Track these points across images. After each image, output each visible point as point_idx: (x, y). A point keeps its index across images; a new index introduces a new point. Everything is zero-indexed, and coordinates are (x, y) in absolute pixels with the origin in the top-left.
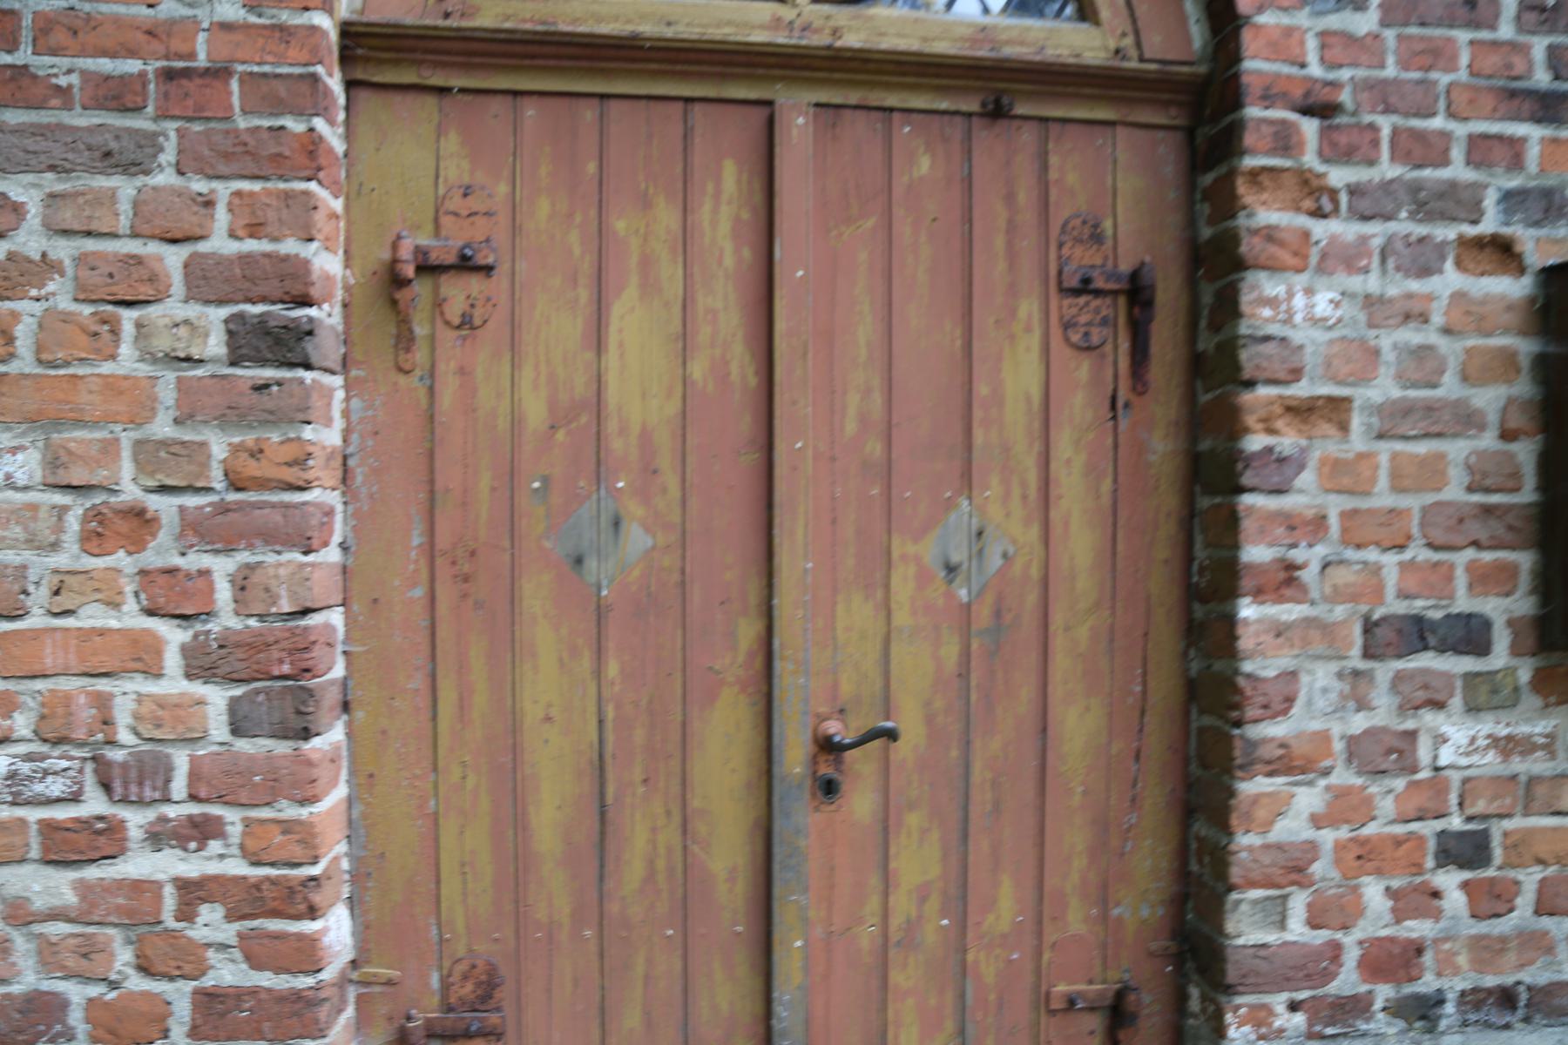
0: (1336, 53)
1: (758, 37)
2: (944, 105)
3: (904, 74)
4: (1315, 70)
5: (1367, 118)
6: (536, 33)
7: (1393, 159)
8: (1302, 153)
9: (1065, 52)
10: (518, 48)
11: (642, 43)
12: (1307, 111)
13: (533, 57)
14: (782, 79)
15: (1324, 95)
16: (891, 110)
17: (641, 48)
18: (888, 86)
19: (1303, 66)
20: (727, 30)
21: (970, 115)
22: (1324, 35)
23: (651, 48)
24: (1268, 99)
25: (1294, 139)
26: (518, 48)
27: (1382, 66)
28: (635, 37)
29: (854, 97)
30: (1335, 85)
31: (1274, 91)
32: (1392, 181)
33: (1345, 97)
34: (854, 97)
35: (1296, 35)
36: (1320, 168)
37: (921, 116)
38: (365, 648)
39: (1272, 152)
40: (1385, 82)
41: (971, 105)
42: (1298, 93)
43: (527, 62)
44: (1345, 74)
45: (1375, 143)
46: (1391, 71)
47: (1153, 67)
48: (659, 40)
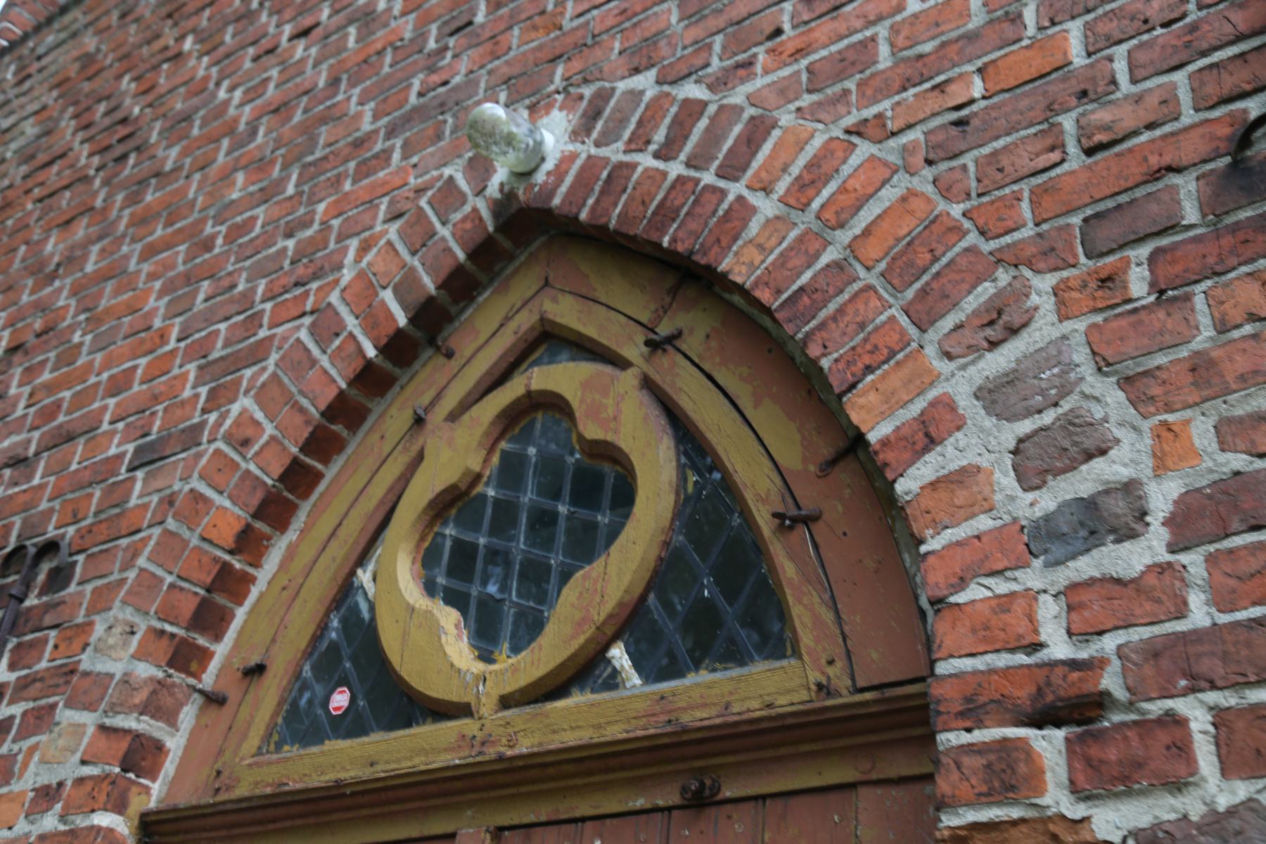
0: (1096, 612)
1: (440, 761)
2: (640, 803)
3: (590, 773)
4: (1059, 648)
5: (1155, 708)
6: (266, 796)
7: (1227, 771)
8: (1040, 790)
9: (755, 704)
10: (259, 815)
11: (342, 791)
12: (1040, 720)
13: (274, 821)
14: (470, 804)
15: (1073, 684)
16: (583, 820)
17: (344, 795)
18: (578, 790)
19: (1037, 646)
20: (699, 714)
21: (669, 809)
22: (1073, 595)
23: (353, 794)
24: (972, 715)
25: (1022, 768)
26: (259, 815)
27: (1181, 611)
28: (338, 784)
29: (543, 812)
30: (1094, 665)
31: (982, 699)
32: (1232, 812)
33: (1111, 682)
34: (543, 812)
35: (1019, 607)
36: (1075, 811)
37: (615, 821)
38: (67, 828)
39: (987, 798)
40: (1195, 636)
41: (668, 796)
42: (1023, 694)
43: (271, 827)
44: (1110, 643)
45: (1182, 749)
46: (1200, 614)
47: (868, 696)
48: (358, 783)
